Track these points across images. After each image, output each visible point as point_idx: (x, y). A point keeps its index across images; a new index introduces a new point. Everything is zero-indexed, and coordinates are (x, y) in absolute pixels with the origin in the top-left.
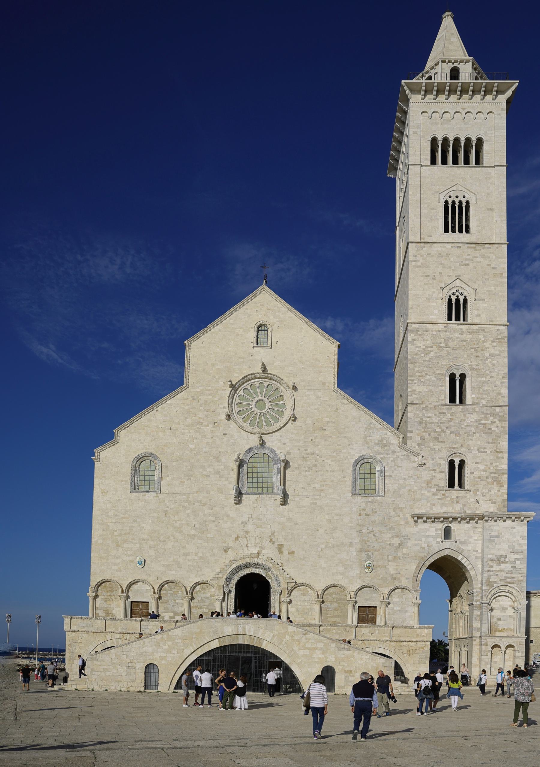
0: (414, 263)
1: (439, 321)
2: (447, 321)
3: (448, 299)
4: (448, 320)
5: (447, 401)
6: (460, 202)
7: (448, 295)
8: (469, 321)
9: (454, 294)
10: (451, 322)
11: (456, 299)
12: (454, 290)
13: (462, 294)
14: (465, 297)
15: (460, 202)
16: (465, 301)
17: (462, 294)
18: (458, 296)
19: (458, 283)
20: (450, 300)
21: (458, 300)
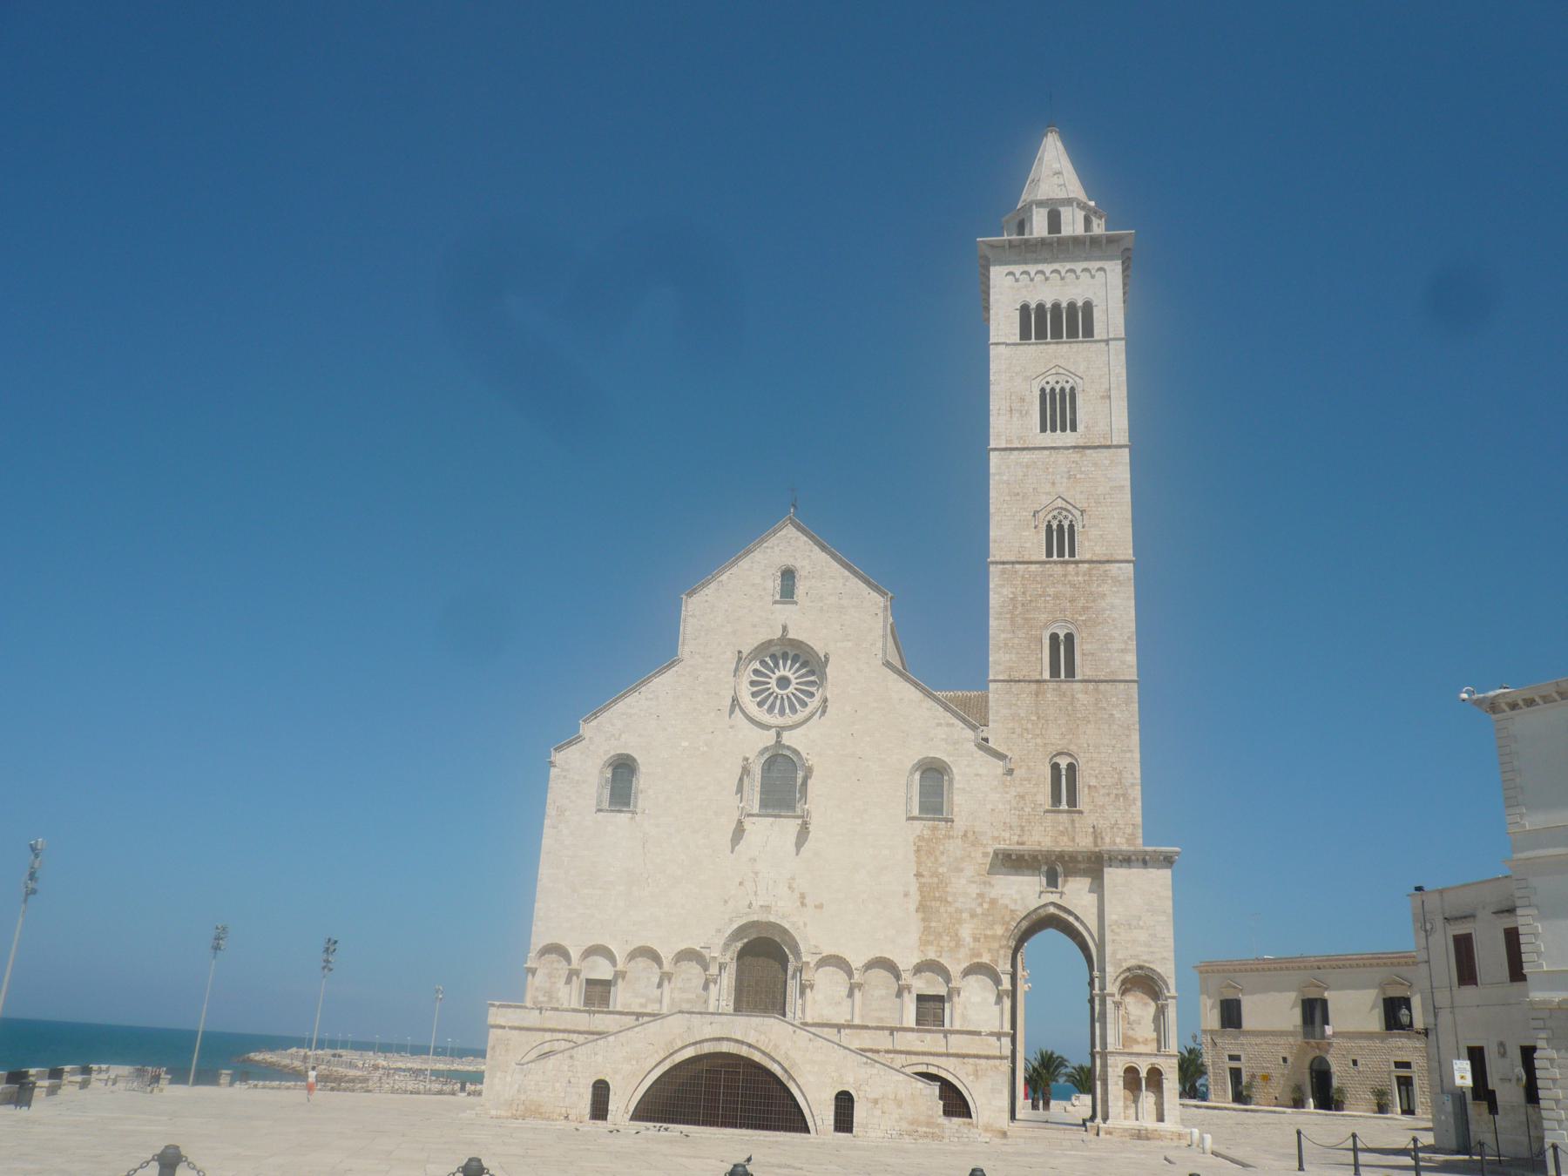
0: (997, 477)
1: (1034, 558)
2: (1044, 558)
3: (1047, 526)
4: (1047, 556)
5: (1046, 675)
6: (1063, 390)
7: (1047, 519)
8: (1077, 558)
9: (1054, 517)
10: (1051, 559)
11: (1058, 526)
12: (1055, 513)
13: (1066, 517)
14: (1071, 521)
15: (1063, 390)
16: (1071, 526)
17: (1066, 517)
18: (1060, 521)
19: (1060, 503)
20: (1049, 527)
21: (1060, 527)
